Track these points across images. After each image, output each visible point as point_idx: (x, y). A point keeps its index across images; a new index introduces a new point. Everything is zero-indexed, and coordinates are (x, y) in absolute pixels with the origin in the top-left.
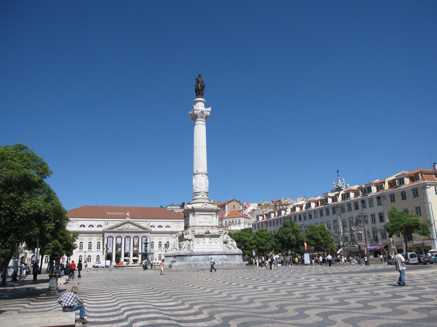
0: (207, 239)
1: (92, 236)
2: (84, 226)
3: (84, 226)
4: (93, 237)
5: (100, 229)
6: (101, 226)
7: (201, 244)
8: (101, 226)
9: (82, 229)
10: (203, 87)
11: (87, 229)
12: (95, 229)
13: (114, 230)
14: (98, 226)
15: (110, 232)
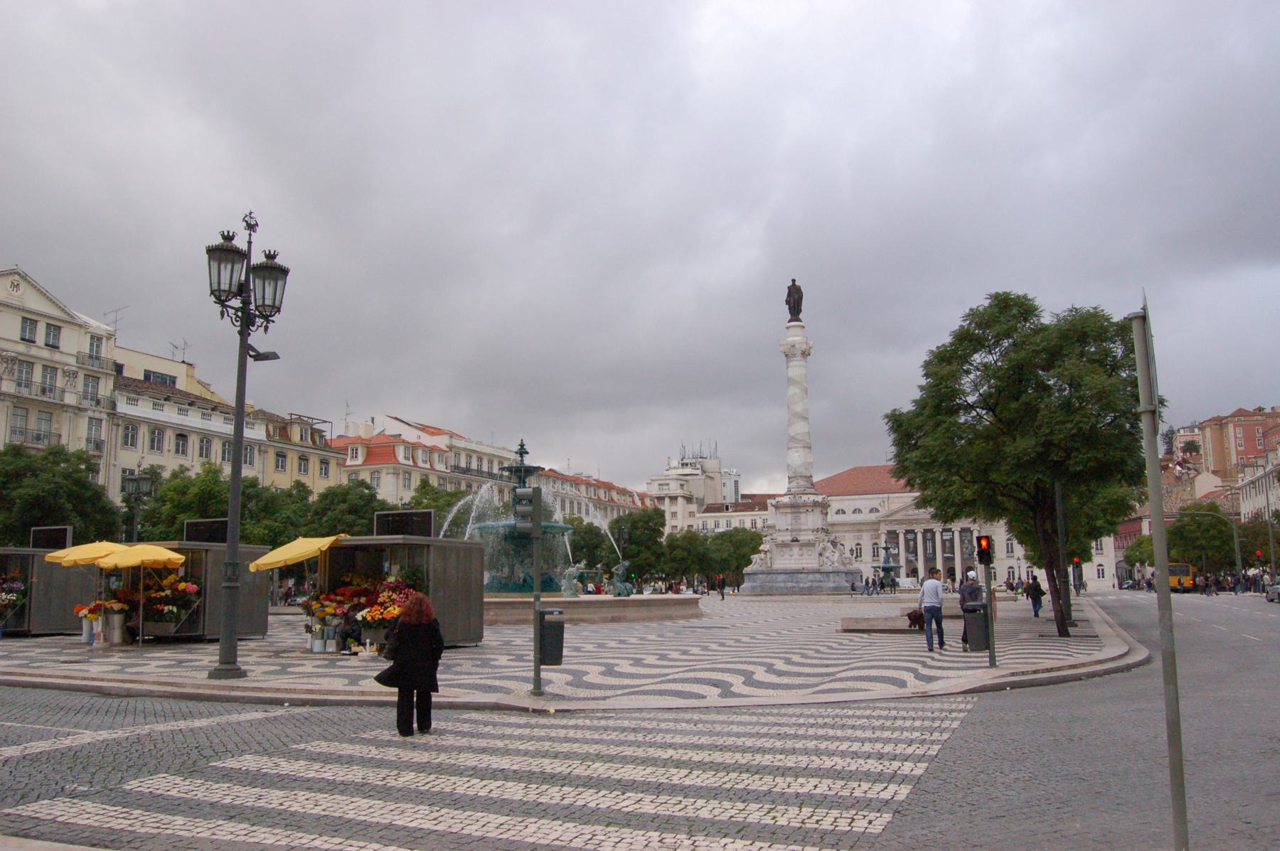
0: (796, 550)
1: (860, 531)
2: (844, 512)
3: (844, 512)
4: (864, 534)
5: (873, 517)
6: (877, 511)
7: (787, 557)
8: (877, 511)
9: (840, 518)
10: (801, 298)
11: (850, 517)
12: (867, 517)
13: (898, 516)
14: (871, 511)
15: (891, 522)
